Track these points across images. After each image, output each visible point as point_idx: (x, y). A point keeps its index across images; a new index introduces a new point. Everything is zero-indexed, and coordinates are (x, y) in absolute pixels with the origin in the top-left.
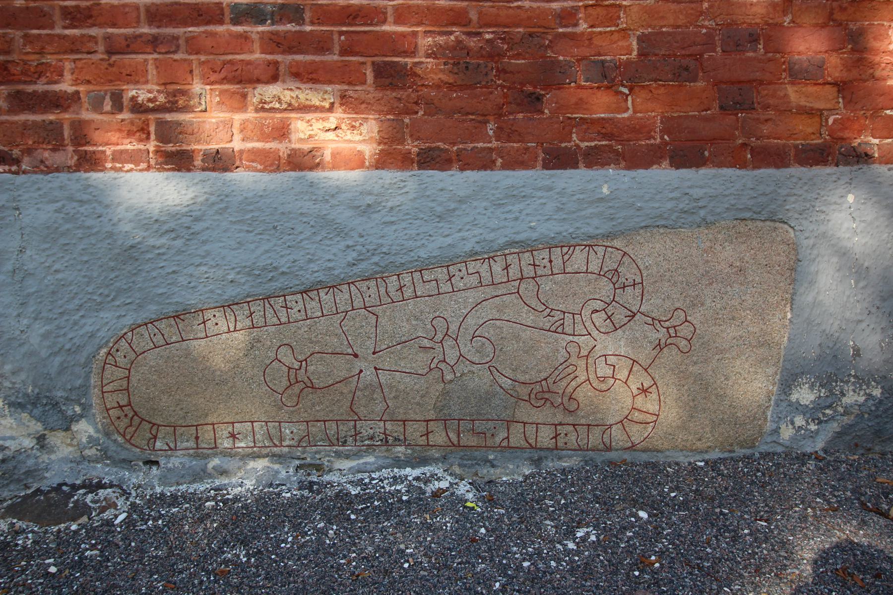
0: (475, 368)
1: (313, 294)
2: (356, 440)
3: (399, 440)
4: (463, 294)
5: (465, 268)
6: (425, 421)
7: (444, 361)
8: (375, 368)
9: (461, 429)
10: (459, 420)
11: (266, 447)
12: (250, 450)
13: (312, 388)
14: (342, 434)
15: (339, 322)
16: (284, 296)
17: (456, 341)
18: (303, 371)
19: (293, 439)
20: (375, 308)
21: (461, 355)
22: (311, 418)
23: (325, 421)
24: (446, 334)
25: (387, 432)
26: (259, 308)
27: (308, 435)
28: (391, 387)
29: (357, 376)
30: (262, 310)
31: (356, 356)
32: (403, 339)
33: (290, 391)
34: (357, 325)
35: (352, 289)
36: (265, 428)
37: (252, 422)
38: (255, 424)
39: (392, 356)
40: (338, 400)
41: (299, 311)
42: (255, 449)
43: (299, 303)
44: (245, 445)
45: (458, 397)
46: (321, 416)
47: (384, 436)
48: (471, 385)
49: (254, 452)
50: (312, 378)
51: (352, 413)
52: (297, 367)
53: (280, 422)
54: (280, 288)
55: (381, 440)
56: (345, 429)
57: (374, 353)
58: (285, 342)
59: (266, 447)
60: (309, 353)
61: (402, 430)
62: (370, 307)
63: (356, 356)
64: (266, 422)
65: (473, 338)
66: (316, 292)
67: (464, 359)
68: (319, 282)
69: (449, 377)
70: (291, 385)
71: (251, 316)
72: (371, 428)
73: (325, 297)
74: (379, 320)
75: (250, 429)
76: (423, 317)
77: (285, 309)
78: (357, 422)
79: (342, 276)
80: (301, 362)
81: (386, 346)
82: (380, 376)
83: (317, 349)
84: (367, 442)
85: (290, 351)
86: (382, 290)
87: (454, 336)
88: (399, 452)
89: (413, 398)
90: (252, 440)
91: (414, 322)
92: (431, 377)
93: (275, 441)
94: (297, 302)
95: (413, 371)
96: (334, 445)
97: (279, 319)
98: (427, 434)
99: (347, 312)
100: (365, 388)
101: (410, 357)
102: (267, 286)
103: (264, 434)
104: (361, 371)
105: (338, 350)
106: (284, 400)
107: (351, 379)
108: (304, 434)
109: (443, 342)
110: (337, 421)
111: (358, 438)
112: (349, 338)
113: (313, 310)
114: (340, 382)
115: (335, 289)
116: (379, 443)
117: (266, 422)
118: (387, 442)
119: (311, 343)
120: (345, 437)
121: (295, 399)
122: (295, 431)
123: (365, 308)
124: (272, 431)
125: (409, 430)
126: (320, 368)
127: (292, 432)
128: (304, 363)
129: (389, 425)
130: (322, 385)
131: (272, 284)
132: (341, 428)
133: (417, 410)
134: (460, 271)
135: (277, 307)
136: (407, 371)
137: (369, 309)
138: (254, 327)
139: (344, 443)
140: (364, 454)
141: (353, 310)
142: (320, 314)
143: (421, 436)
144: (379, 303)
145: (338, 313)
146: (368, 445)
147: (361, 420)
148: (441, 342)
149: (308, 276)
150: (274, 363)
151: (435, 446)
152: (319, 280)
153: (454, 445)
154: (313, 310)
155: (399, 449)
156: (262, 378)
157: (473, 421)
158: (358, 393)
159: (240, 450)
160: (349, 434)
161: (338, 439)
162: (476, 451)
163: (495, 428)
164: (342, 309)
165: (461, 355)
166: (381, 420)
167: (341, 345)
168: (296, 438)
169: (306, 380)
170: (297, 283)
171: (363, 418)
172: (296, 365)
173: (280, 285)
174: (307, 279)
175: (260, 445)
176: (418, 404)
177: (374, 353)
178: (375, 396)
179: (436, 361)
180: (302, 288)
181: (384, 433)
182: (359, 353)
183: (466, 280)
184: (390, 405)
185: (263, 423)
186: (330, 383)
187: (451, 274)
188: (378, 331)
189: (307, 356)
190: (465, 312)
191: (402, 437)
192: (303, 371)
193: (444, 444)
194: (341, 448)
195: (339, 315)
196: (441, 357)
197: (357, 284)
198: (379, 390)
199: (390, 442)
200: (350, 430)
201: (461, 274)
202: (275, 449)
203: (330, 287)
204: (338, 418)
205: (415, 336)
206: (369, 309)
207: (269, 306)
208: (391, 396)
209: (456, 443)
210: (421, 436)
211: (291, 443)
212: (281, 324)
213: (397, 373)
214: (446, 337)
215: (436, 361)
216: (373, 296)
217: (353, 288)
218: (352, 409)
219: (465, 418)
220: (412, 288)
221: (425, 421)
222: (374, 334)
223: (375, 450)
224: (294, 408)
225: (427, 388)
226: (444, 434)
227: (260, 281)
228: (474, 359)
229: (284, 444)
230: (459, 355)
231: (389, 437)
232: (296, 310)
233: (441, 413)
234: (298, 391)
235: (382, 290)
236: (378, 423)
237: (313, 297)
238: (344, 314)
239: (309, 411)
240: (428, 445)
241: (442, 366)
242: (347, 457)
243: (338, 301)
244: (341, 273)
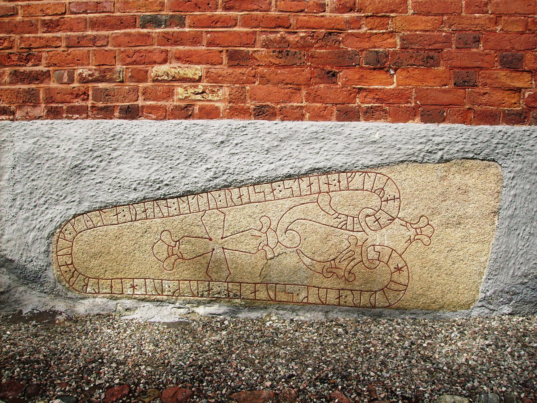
3: (237, 295)
6: (253, 283)
7: (267, 245)
8: (223, 248)
12: (143, 297)
13: (183, 259)
14: (201, 289)
18: (177, 248)
31: (211, 239)
33: (168, 260)
35: (209, 196)
36: (152, 283)
42: (146, 296)
51: (207, 277)
53: (162, 280)
57: (222, 238)
61: (239, 289)
63: (211, 239)
84: (216, 296)
85: (169, 236)
88: (237, 303)
96: (195, 296)
98: (255, 292)
104: (214, 249)
116: (224, 296)
118: (229, 296)
123: (217, 209)
126: (188, 247)
138: (147, 219)
142: (188, 212)
147: (213, 281)
148: (266, 233)
154: (184, 209)
155: (237, 300)
157: (285, 285)
159: (138, 296)
160: (205, 289)
161: (198, 293)
166: (225, 282)
172: (173, 244)
177: (222, 238)
182: (212, 238)
184: (231, 272)
191: (238, 294)
192: (177, 248)
194: (200, 298)
195: (200, 213)
196: (265, 242)
202: (159, 297)
221: (253, 283)
223: (221, 301)
224: (171, 272)
226: (266, 293)
228: (287, 245)
232: (173, 208)
241: (266, 248)
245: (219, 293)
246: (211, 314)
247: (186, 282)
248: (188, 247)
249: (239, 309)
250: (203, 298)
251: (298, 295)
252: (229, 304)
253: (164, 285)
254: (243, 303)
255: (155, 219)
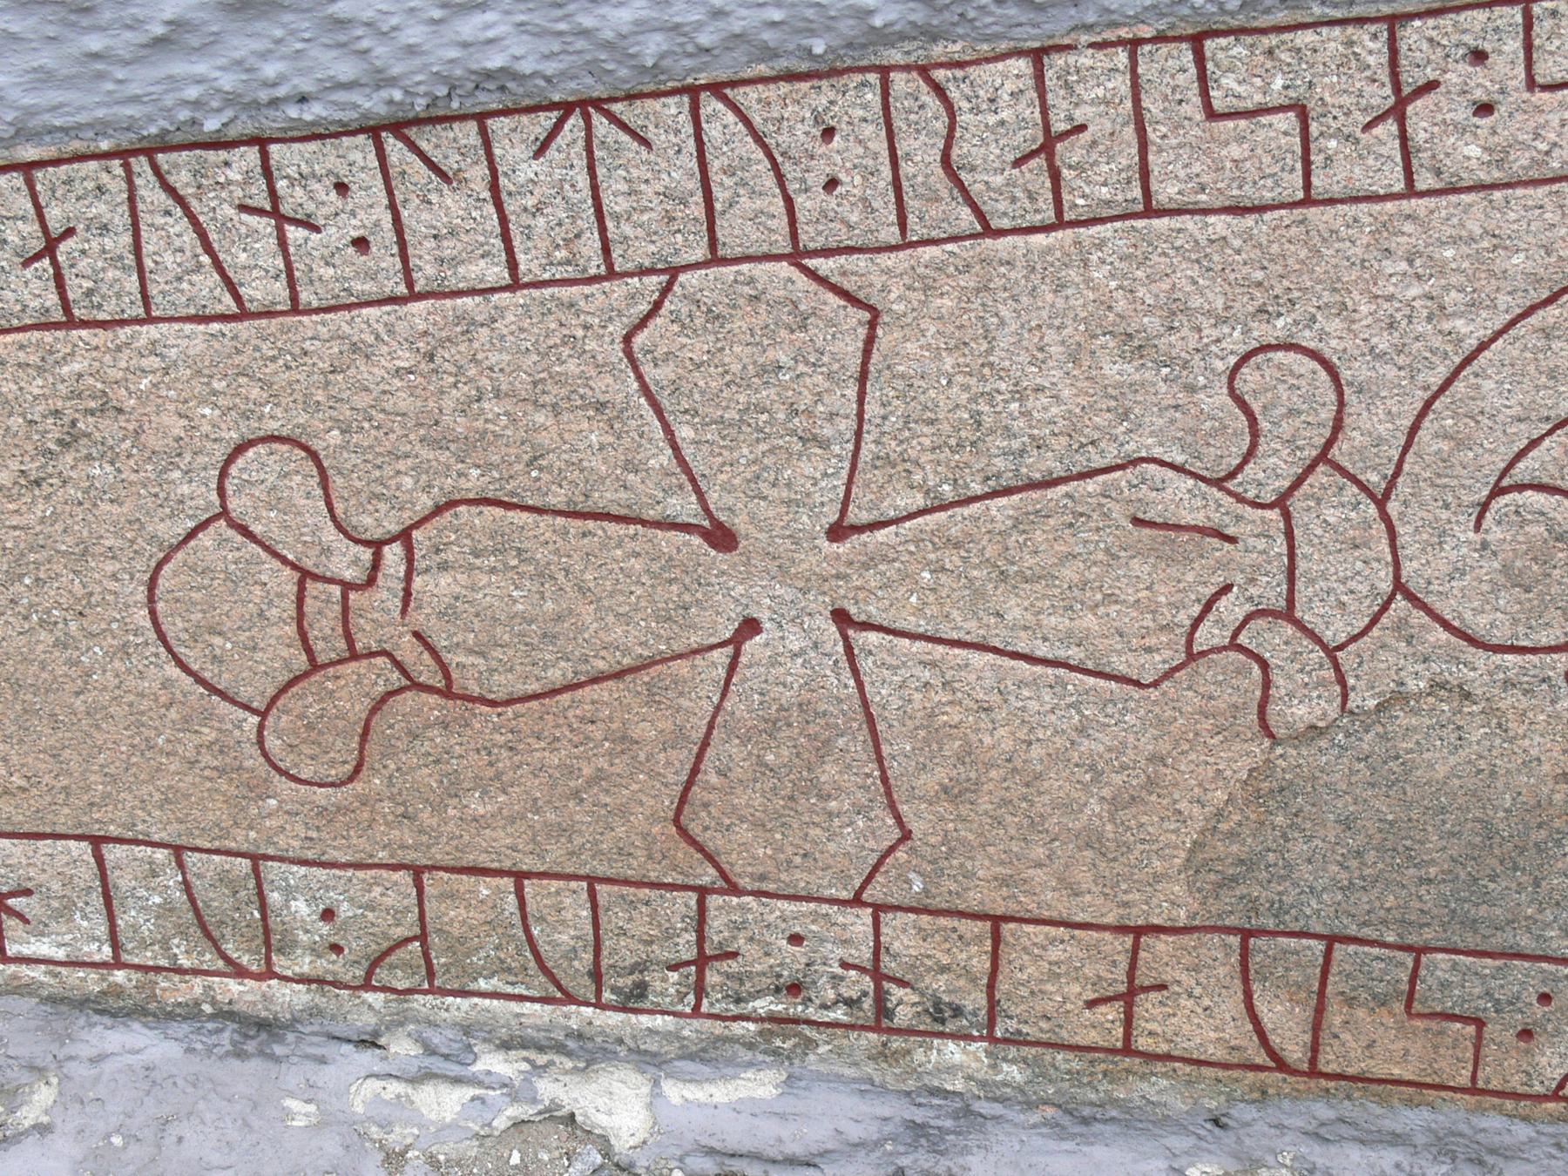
0: (1478, 669)
1: (439, 142)
2: (700, 990)
3: (958, 1011)
4: (1474, 213)
5: (1514, 45)
6: (1121, 929)
7: (1288, 613)
8: (841, 617)
9: (1335, 984)
10: (1331, 940)
11: (180, 971)
12: (92, 982)
13: (447, 693)
14: (619, 951)
15: (617, 329)
16: (261, 142)
17: (1381, 503)
18: (386, 594)
19: (336, 948)
20: (860, 262)
21: (1399, 586)
22: (439, 855)
23: (520, 876)
24: (1323, 457)
25: (889, 965)
26: (100, 209)
27: (423, 937)
28: (932, 732)
29: (721, 656)
30: (121, 219)
31: (721, 537)
32: (1038, 465)
33: (305, 700)
34: (737, 357)
35: (712, 131)
36: (172, 879)
37: (97, 842)
38: (113, 853)
39: (952, 559)
40: (599, 777)
41: (361, 244)
42: (119, 976)
43: (358, 197)
44: (61, 954)
45: (1347, 824)
46: (498, 846)
47: (868, 983)
48: (1441, 763)
49: (117, 991)
50: (441, 642)
51: (683, 851)
52: (349, 575)
53: (256, 858)
54: (231, 99)
55: (850, 1003)
56: (640, 927)
57: (837, 532)
58: (272, 426)
59: (180, 971)
60: (425, 502)
61: (982, 964)
62: (826, 252)
63: (721, 537)
64: (178, 851)
65: (1498, 491)
66: (467, 133)
67: (1419, 617)
68: (489, 75)
69: (1297, 712)
70: (315, 666)
71: (50, 249)
72: (796, 939)
73: (527, 170)
74: (886, 338)
75: (87, 873)
76: (1180, 342)
77: (265, 225)
78: (714, 901)
79: (652, 47)
80: (377, 545)
81: (920, 501)
82: (865, 664)
83: (474, 482)
84: (762, 1005)
85: (302, 486)
86: (921, 154)
87: (1373, 478)
88: (951, 1069)
89: (1068, 807)
90: (102, 930)
91: (1112, 370)
92: (1191, 700)
93: (229, 947)
94: (342, 188)
95: (1075, 654)
96: (570, 999)
97: (231, 287)
98: (1129, 997)
99: (674, 272)
100: (772, 727)
101: (1069, 573)
102: (141, 79)
103: (167, 908)
104: (750, 626)
105: (605, 498)
106: (273, 743)
107: (681, 668)
108: (399, 932)
109: (1296, 504)
110: (592, 880)
111: (712, 978)
112: (684, 433)
113: (450, 248)
114: (618, 675)
115: (599, 121)
116: (839, 1014)
117: (178, 851)
118: (883, 1009)
119: (437, 444)
120: (640, 967)
121: (344, 751)
122: (345, 910)
123: (796, 256)
124: (216, 901)
125: (1021, 970)
126: (493, 591)
127: (328, 915)
128: (393, 554)
129: (902, 935)
130: (502, 685)
131: (179, 67)
132: (614, 918)
133: (1083, 877)
134: (1479, 56)
135: (218, 210)
136: (1042, 651)
137: (823, 265)
138: (71, 323)
139: (633, 999)
140: (747, 1056)
141: (715, 259)
142: (496, 273)
143: (1091, 1004)
144: (891, 234)
145: (611, 274)
146: (772, 1018)
147: (734, 889)
148: (1281, 502)
149: (413, 34)
150: (205, 539)
151: (1167, 1057)
152: (495, 61)
153: (1281, 1065)
154: (450, 248)
155: (953, 1051)
156: (141, 617)
157: (1419, 951)
158: (724, 750)
160: (663, 954)
161: (596, 975)
162: (1409, 1103)
163: (1545, 998)
164: (643, 253)
165: (1399, 586)
166: (857, 901)
167: (631, 466)
168: (355, 945)
169: (408, 650)
170: (346, 69)
171: (745, 882)
172: (347, 561)
173: (228, 82)
174: (412, 50)
175: (147, 957)
176: (1091, 840)
177: (837, 532)
178: (829, 772)
179: (1231, 609)
180: (374, 104)
181: (877, 974)
182: (740, 523)
183: (1507, 125)
184: (916, 826)
185: (161, 855)
186: (556, 675)
187: (1412, 77)
188: (872, 409)
189: (408, 517)
190: (1471, 330)
191: (975, 1000)
192: (386, 594)
193: (1220, 1054)
194: (615, 1018)
195: (617, 289)
196: (1271, 592)
197: (748, 97)
198: (858, 746)
199: (903, 1016)
200: (669, 935)
201: (1482, 83)
202: (234, 986)
203: (567, 108)
204: (602, 870)
205: (1111, 455)
206: (823, 265)
207: (161, 197)
208: (929, 782)
209: (1295, 1053)
210: (1091, 1004)
211: (327, 965)
212: (243, 315)
213: (978, 659)
214: (1322, 475)
215: (1231, 609)
216: (852, 184)
217: (719, 120)
218: (683, 832)
219: (1367, 932)
220: (1129, 154)
221: (1121, 929)
222: (847, 426)
223: (810, 1044)
224: (336, 795)
225: (1157, 759)
226: (1232, 1004)
227: (95, 43)
228: (1479, 624)
229: (280, 963)
230: (1386, 586)
231: (897, 992)
232: (336, 235)
233: (1228, 897)
234: (361, 708)
235: (921, 154)
236: (840, 916)
237: (451, 163)
238: (654, 281)
239: (426, 817)
240: (1128, 1050)
241: (1274, 640)
242: (649, 1060)
243: (615, 203)
244: (643, 27)
245: (795, 988)
246: (711, 1152)
247: (484, 888)
248: (493, 591)
249: (967, 1111)
250: (645, 1020)
251: (1526, 1034)
252: (888, 1075)
253: (274, 897)
254: (1014, 1073)
255: (150, 332)
